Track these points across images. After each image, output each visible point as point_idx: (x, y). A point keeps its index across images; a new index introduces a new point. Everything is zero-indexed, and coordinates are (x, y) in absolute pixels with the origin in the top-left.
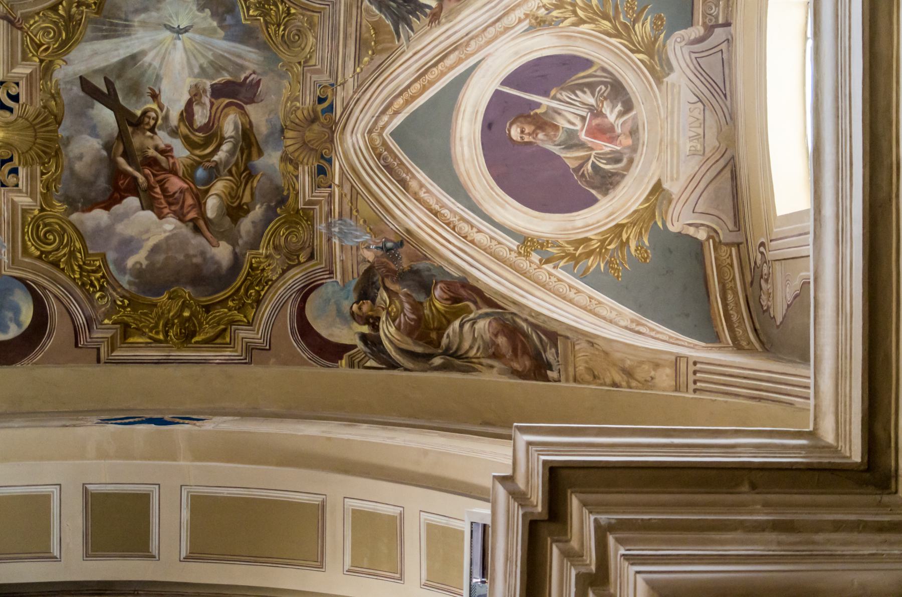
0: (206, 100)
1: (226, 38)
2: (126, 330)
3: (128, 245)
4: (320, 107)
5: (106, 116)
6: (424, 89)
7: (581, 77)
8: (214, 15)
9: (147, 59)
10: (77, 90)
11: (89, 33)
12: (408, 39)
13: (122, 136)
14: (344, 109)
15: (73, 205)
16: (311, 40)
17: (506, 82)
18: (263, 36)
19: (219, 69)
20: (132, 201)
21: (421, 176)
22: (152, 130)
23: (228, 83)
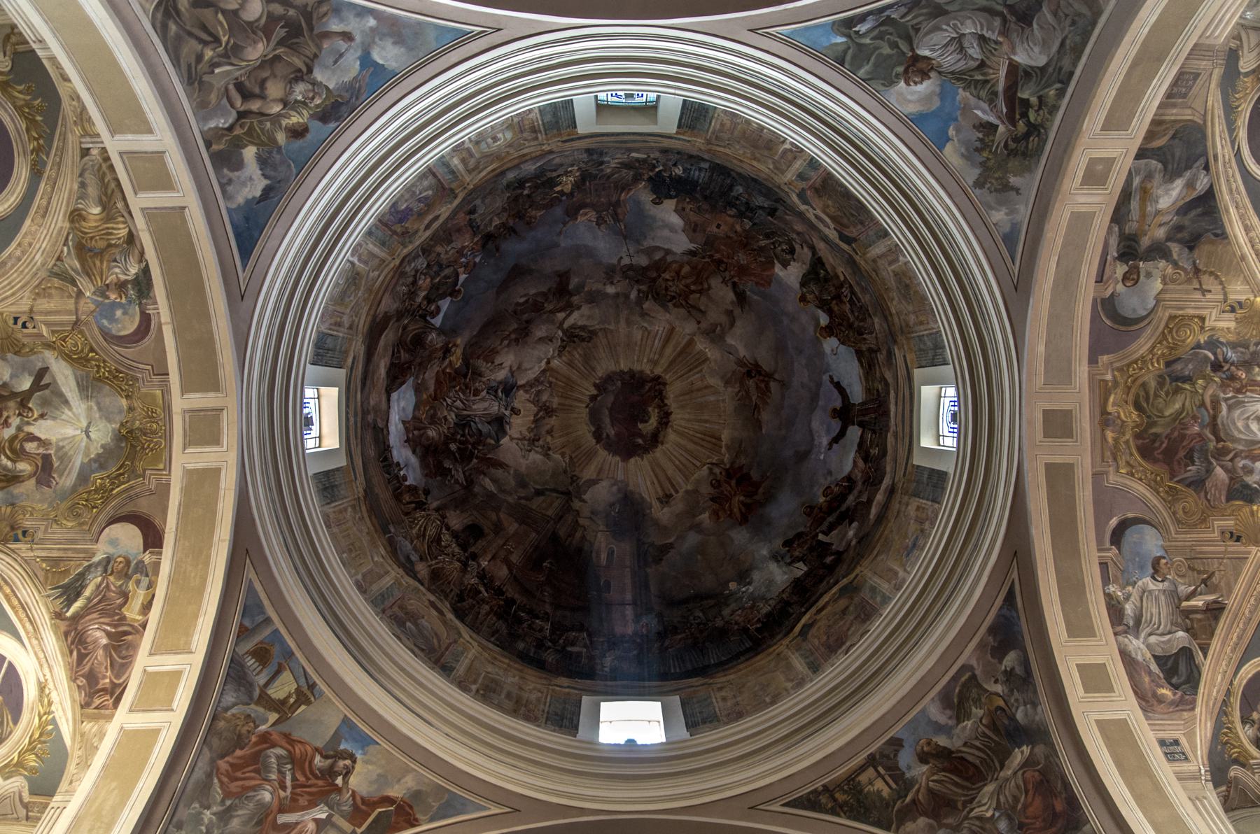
0: (41, 451)
1: (82, 464)
4: (20, 532)
5: (26, 384)
6: (13, 607)
8: (99, 455)
9: (66, 411)
10: (39, 365)
11: (79, 373)
12: (48, 596)
13: (14, 395)
14: (13, 550)
16: (70, 524)
17: (10, 664)
18: (81, 490)
19: (61, 459)
22: (20, 414)
23: (52, 465)
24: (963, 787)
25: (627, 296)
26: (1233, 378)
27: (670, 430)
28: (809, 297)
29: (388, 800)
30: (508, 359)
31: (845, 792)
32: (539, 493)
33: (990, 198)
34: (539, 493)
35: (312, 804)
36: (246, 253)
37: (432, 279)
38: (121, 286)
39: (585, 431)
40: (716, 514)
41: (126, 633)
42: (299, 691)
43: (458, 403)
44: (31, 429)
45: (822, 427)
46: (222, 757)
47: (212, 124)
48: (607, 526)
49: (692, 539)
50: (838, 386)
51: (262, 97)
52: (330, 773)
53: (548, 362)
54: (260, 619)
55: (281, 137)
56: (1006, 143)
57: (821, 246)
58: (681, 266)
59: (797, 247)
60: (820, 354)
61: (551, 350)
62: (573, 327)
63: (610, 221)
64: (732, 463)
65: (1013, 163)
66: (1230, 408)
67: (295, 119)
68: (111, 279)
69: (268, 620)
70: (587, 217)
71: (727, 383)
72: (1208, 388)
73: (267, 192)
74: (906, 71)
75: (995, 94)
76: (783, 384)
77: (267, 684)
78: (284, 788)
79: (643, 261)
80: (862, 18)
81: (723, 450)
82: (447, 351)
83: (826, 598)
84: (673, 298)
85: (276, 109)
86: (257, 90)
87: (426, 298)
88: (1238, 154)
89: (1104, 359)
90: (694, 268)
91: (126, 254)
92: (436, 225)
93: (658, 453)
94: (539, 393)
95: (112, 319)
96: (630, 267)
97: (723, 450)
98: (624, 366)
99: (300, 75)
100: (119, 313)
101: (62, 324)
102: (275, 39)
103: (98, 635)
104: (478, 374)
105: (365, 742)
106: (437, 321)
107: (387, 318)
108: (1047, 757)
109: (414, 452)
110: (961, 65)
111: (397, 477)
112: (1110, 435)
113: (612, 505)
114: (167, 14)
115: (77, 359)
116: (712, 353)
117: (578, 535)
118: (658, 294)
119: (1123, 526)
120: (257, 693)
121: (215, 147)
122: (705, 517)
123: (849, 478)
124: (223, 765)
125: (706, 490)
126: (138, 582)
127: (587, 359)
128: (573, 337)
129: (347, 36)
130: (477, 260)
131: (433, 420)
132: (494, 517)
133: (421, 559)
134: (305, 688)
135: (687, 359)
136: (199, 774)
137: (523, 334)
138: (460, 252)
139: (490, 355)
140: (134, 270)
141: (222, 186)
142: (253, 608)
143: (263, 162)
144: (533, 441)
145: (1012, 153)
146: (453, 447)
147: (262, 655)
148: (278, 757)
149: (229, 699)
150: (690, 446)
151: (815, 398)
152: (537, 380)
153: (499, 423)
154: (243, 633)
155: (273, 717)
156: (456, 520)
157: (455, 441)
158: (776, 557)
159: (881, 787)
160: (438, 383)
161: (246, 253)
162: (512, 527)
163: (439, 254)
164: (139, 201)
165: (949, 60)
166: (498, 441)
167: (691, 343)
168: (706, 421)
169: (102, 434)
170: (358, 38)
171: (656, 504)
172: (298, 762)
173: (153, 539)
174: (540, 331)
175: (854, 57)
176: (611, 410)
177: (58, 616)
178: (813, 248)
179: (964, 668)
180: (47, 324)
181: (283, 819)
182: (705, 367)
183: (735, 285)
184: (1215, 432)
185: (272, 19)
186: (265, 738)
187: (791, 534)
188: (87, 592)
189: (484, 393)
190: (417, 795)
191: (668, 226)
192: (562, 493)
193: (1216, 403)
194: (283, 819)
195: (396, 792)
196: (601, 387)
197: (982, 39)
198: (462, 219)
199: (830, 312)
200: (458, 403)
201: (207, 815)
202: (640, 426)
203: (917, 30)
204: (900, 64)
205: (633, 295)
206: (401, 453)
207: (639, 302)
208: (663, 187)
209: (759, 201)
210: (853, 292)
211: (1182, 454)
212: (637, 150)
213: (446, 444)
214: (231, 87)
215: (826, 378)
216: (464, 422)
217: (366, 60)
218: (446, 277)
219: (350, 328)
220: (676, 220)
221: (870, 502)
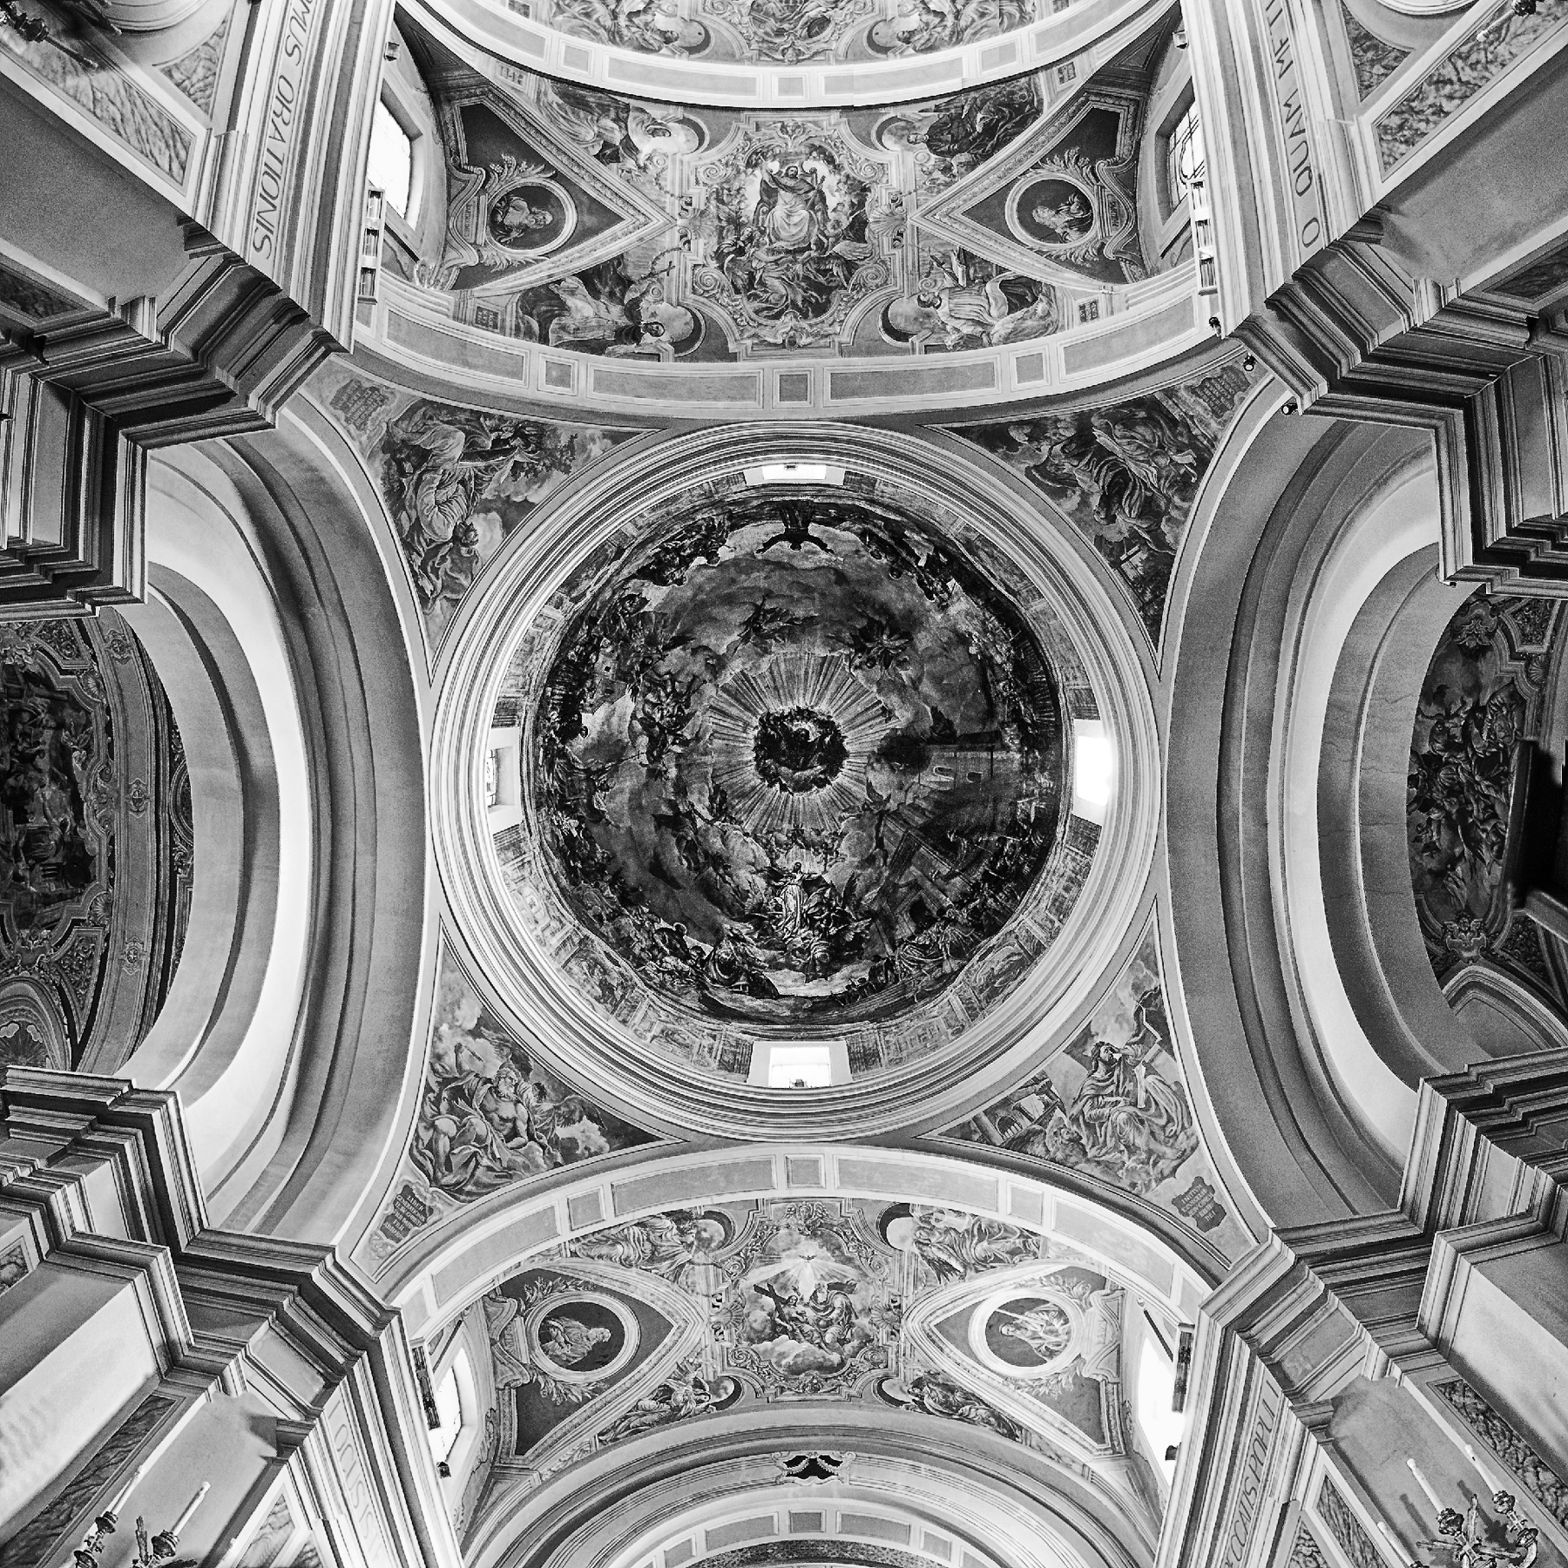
2: (782, 1389)
3: (782, 1355)
5: (769, 1302)
7: (1042, 1307)
15: (752, 1341)
20: (785, 1337)
21: (952, 1347)
24: (1134, 488)
25: (679, 756)
26: (750, 238)
27: (816, 709)
28: (677, 576)
29: (1137, 1013)
30: (744, 876)
31: (1144, 592)
32: (880, 844)
33: (580, 458)
34: (880, 844)
35: (1133, 1078)
36: (648, 1138)
37: (665, 954)
38: (682, 1232)
39: (818, 796)
40: (902, 664)
41: (980, 1229)
43: (789, 926)
44: (806, 1299)
45: (810, 558)
46: (1085, 1153)
47: (541, 1161)
48: (914, 774)
49: (926, 687)
50: (767, 545)
51: (514, 1120)
52: (1110, 1065)
53: (746, 835)
54: (974, 1126)
55: (547, 1106)
56: (533, 452)
57: (625, 573)
58: (647, 702)
59: (628, 592)
60: (735, 562)
61: (734, 832)
62: (710, 810)
63: (604, 778)
64: (850, 646)
65: (549, 444)
66: (778, 239)
67: (530, 1095)
68: (677, 1239)
69: (975, 1119)
70: (600, 800)
71: (766, 651)
72: (760, 257)
73: (591, 1118)
74: (465, 545)
75: (486, 468)
76: (768, 594)
77: (1030, 1119)
78: (1117, 1102)
79: (643, 740)
80: (421, 589)
81: (836, 654)
82: (737, 938)
83: (981, 568)
84: (680, 709)
86: (510, 1125)
87: (685, 962)
89: (732, 347)
90: (649, 689)
91: (654, 1228)
92: (614, 954)
93: (839, 721)
94: (778, 844)
95: (711, 1240)
96: (649, 753)
97: (836, 654)
98: (750, 756)
99: (495, 1090)
100: (704, 1235)
101: (717, 1275)
102: (468, 1109)
103: (981, 1249)
104: (760, 907)
105: (1087, 1034)
106: (708, 949)
107: (704, 1000)
108: (1102, 417)
109: (837, 971)
110: (462, 500)
111: (860, 989)
112: (804, 341)
113: (893, 769)
114: (461, 1191)
115: (746, 1268)
116: (736, 666)
117: (924, 805)
118: (676, 724)
119: (889, 329)
120: (1037, 1127)
121: (560, 1160)
122: (906, 674)
123: (862, 535)
125: (877, 672)
126: (937, 1220)
127: (744, 795)
128: (721, 808)
129: (458, 1048)
130: (646, 910)
131: (805, 951)
132: (904, 890)
133: (940, 966)
134: (1038, 1087)
135: (742, 692)
136: (1097, 1172)
137: (719, 861)
138: (640, 927)
139: (742, 894)
140: (668, 1223)
141: (591, 1155)
142: (964, 1132)
143: (569, 1121)
144: (828, 851)
145: (539, 446)
146: (833, 931)
147: (1005, 1124)
148: (1092, 1107)
149: (1039, 1150)
150: (833, 686)
151: (779, 565)
152: (765, 846)
153: (809, 884)
154: (986, 1139)
156: (906, 928)
157: (827, 929)
158: (943, 607)
159: (1137, 561)
160: (769, 946)
161: (648, 1138)
162: (914, 871)
163: (642, 950)
164: (609, 1219)
165: (457, 510)
166: (827, 886)
167: (724, 689)
168: (806, 673)
169: (811, 1247)
170: (459, 1040)
171: (893, 724)
173: (902, 1210)
174: (717, 844)
175: (453, 591)
176: (795, 770)
177: (962, 1277)
178: (627, 580)
179: (1028, 473)
180: (717, 1284)
182: (750, 674)
183: (667, 648)
184: (802, 251)
185: (452, 1110)
187: (919, 590)
188: (944, 1257)
189: (779, 900)
190: (1136, 988)
191: (608, 719)
192: (880, 820)
193: (773, 251)
195: (1131, 1006)
196: (770, 777)
197: (441, 485)
198: (607, 929)
199: (692, 557)
200: (789, 926)
201: (1130, 1164)
202: (812, 739)
203: (432, 541)
204: (459, 551)
205: (678, 749)
206: (837, 984)
207: (685, 743)
208: (571, 728)
209: (582, 635)
210: (672, 539)
211: (821, 279)
212: (536, 758)
213: (829, 938)
214: (510, 1145)
215: (759, 556)
216: (808, 921)
217: (475, 1033)
218: (664, 941)
219: (714, 1037)
220: (601, 712)
221: (882, 518)
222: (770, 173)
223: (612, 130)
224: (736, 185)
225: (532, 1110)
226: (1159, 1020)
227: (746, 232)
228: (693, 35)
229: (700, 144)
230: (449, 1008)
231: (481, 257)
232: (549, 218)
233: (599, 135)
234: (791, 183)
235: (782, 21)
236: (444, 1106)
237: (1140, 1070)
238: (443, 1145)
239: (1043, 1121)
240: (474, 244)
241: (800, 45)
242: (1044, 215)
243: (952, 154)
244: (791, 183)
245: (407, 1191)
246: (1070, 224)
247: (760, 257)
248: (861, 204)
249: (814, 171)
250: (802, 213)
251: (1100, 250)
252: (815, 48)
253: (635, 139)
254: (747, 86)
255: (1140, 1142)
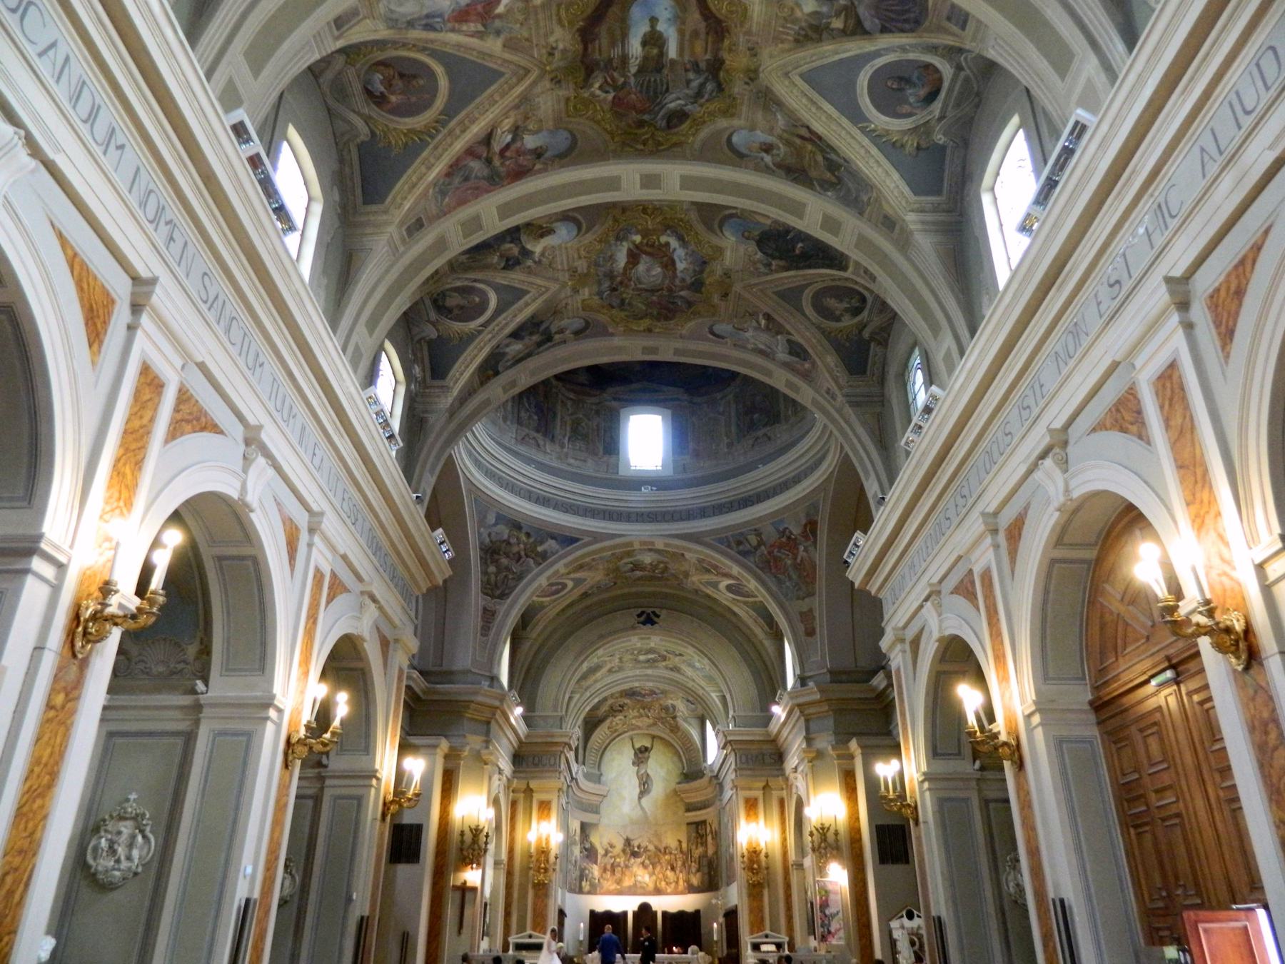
26: (621, 283)
29: (805, 526)
36: (577, 540)
42: (756, 535)
51: (518, 553)
52: (789, 538)
55: (531, 540)
66: (640, 283)
67: (524, 538)
73: (553, 538)
85: (522, 546)
88: (485, 325)
89: (610, 330)
99: (508, 543)
105: (782, 521)
112: (657, 330)
124: (773, 571)
129: (489, 535)
142: (720, 541)
143: (542, 543)
147: (739, 543)
154: (729, 546)
155: (763, 548)
161: (577, 540)
172: (781, 547)
181: (799, 560)
186: (770, 553)
190: (808, 515)
193: (638, 289)
194: (799, 560)
195: (804, 522)
201: (788, 584)
211: (671, 306)
222: (634, 242)
223: (510, 249)
224: (609, 254)
225: (525, 544)
226: (814, 533)
227: (619, 279)
228: (562, 140)
229: (579, 229)
230: (482, 522)
231: (437, 330)
232: (477, 299)
233: (501, 256)
234: (648, 250)
235: (643, 112)
236: (489, 561)
237: (802, 548)
238: (493, 578)
239: (756, 548)
240: (429, 321)
241: (660, 136)
242: (831, 303)
243: (774, 258)
244: (648, 250)
245: (485, 610)
246: (846, 310)
247: (628, 294)
248: (702, 272)
249: (668, 244)
250: (658, 270)
251: (860, 332)
252: (675, 139)
253: (529, 247)
254: (613, 183)
255: (794, 577)
